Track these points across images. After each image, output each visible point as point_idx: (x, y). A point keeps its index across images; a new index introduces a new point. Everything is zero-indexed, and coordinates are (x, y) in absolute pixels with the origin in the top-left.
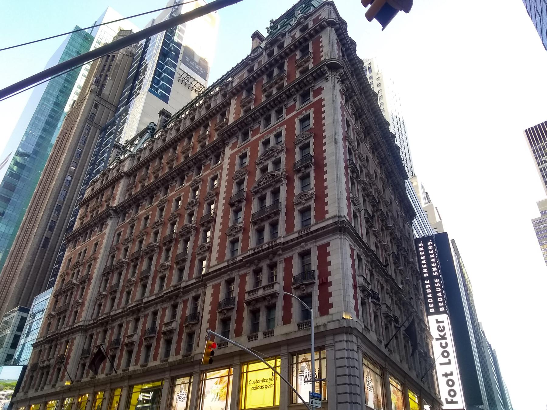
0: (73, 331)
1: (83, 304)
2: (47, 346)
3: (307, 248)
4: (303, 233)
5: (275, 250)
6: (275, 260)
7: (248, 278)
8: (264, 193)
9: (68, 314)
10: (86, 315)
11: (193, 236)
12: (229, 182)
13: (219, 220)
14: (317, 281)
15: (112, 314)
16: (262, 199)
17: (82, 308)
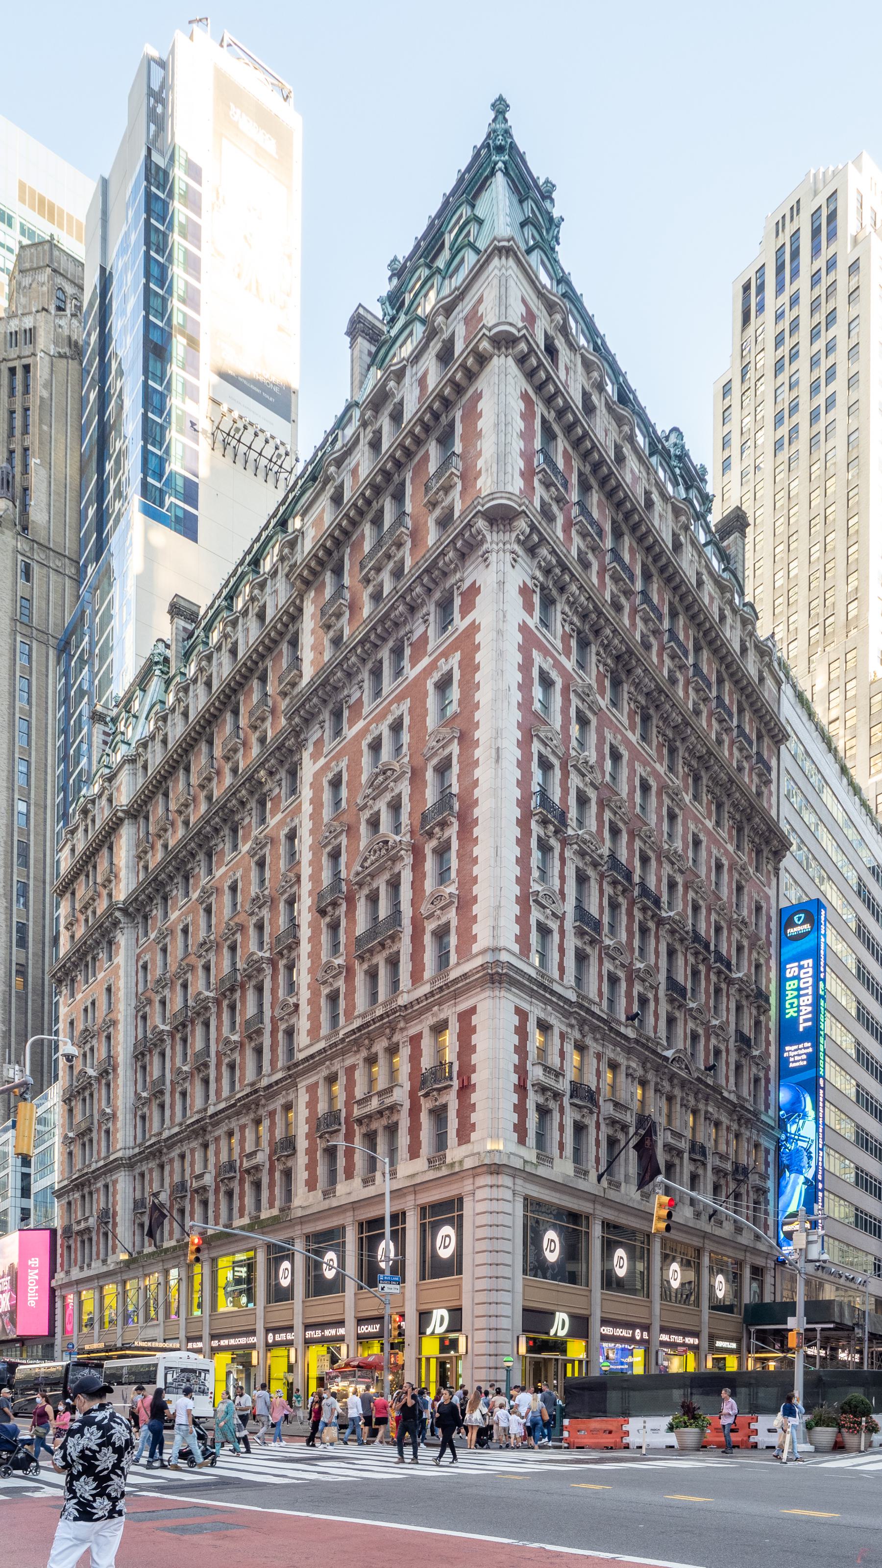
0: (111, 1168)
1: (114, 1115)
2: (77, 1195)
3: (442, 1016)
4: (439, 984)
5: (391, 1021)
6: (395, 1039)
7: (357, 1074)
8: (375, 886)
9: (95, 1135)
10: (124, 1138)
11: (269, 978)
12: (316, 849)
13: (305, 947)
14: (456, 1083)
15: (166, 1134)
16: (373, 899)
17: (114, 1124)
